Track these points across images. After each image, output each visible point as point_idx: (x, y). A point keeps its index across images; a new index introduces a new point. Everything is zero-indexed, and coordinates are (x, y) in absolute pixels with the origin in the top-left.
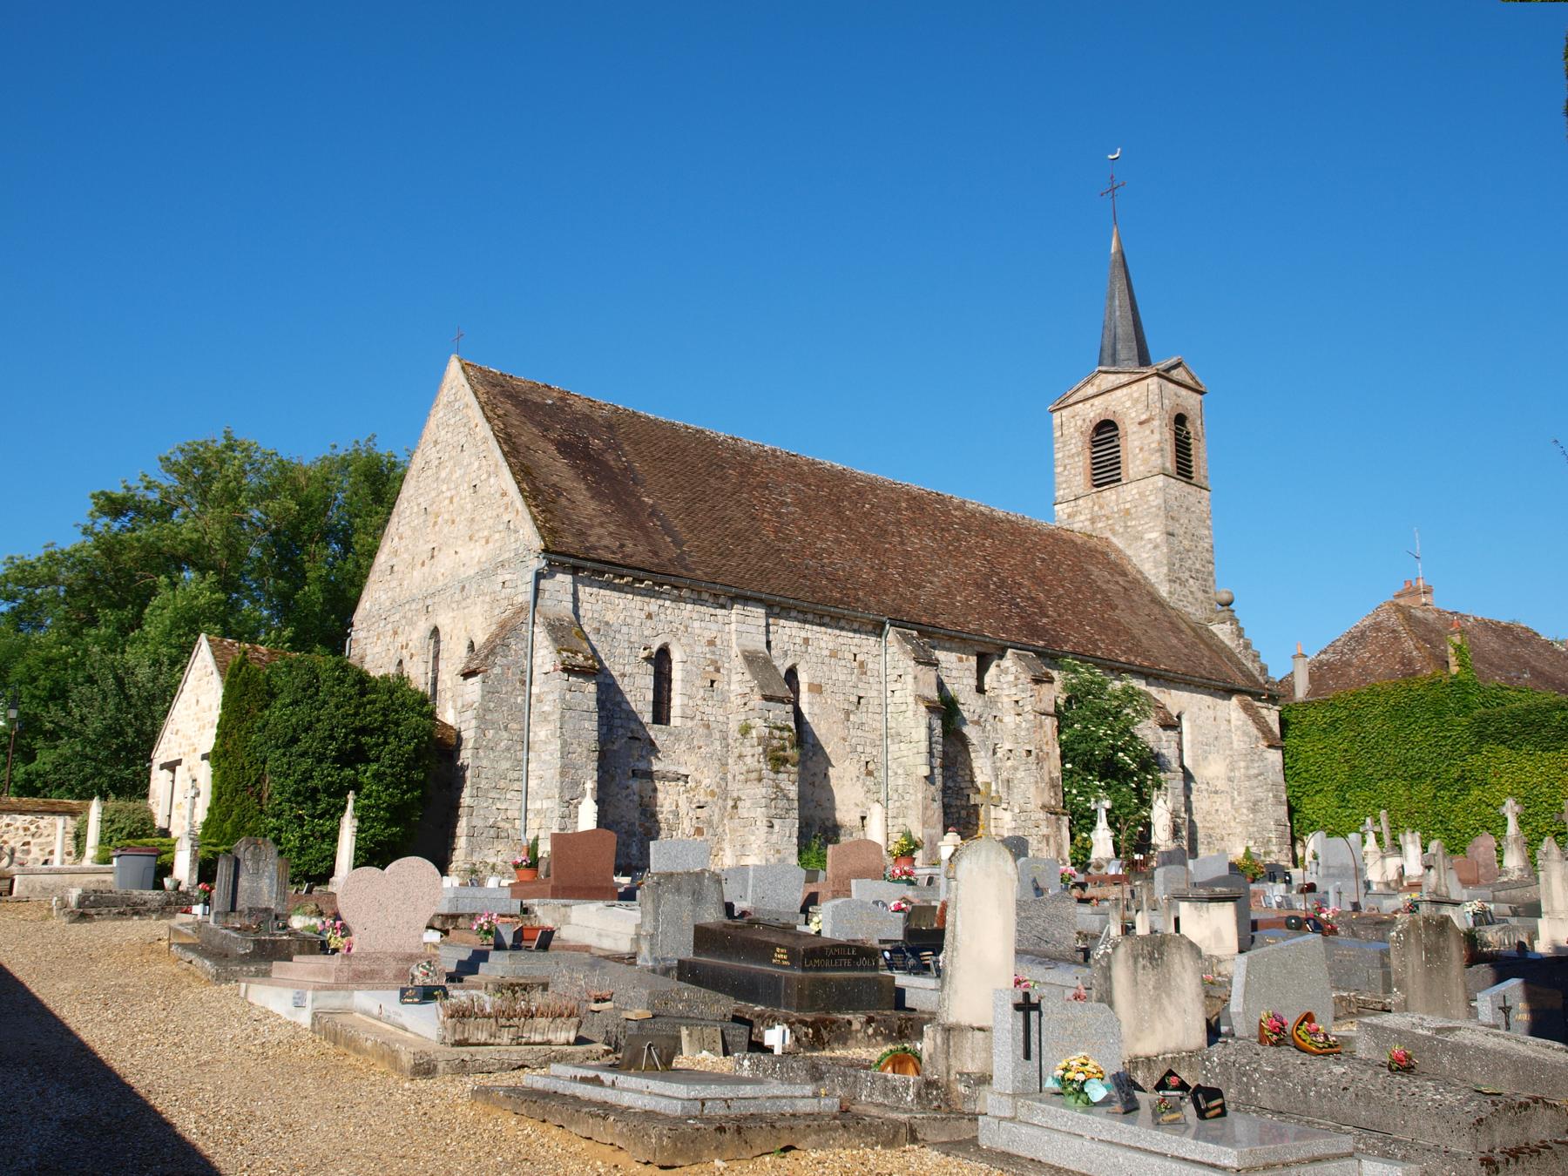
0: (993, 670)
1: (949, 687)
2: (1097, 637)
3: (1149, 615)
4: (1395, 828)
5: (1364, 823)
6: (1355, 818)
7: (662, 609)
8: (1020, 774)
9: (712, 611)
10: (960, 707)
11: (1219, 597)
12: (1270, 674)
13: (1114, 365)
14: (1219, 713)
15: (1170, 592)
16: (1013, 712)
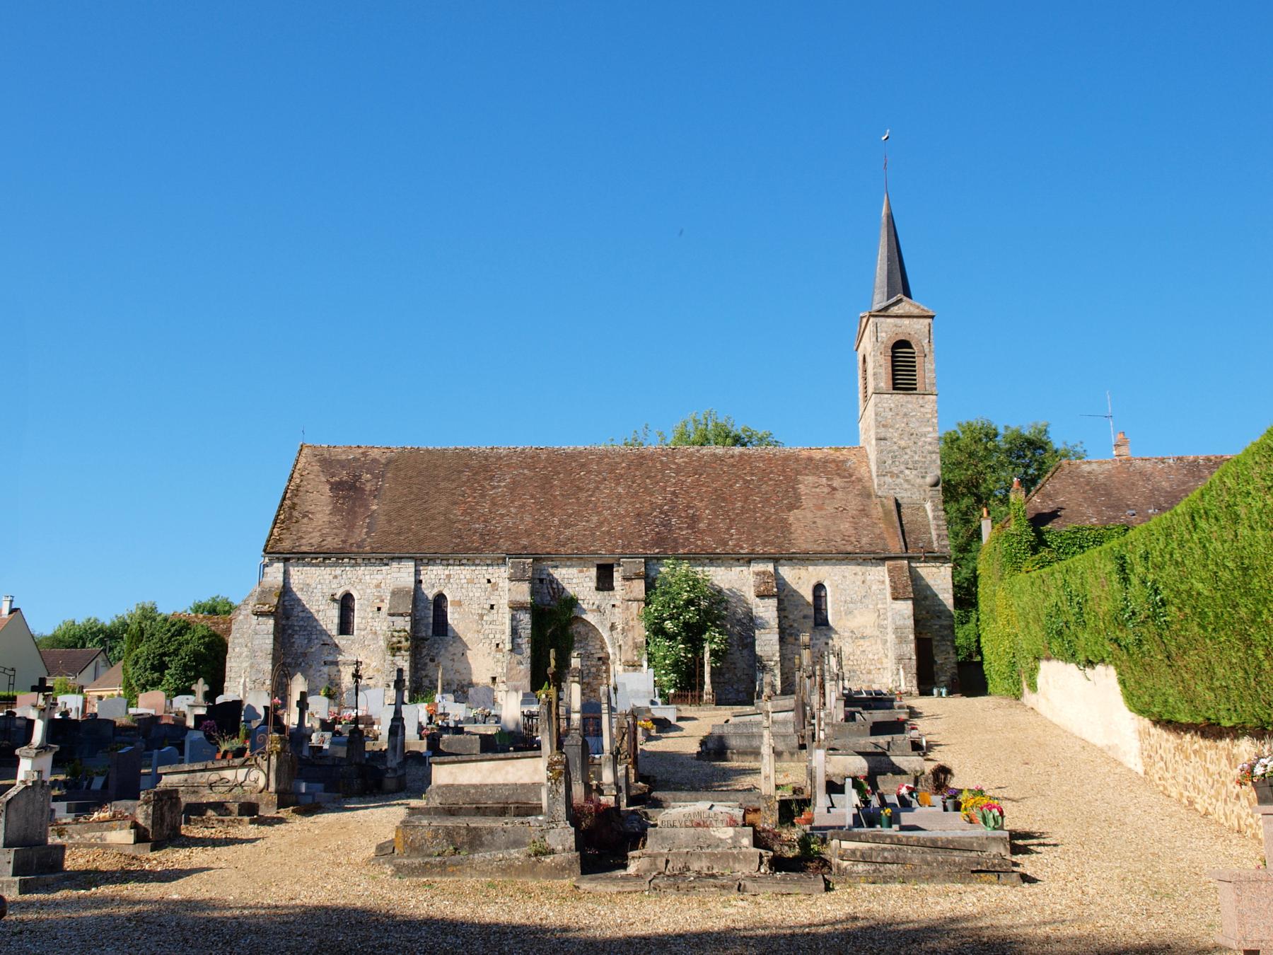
7: (344, 572)
9: (379, 568)
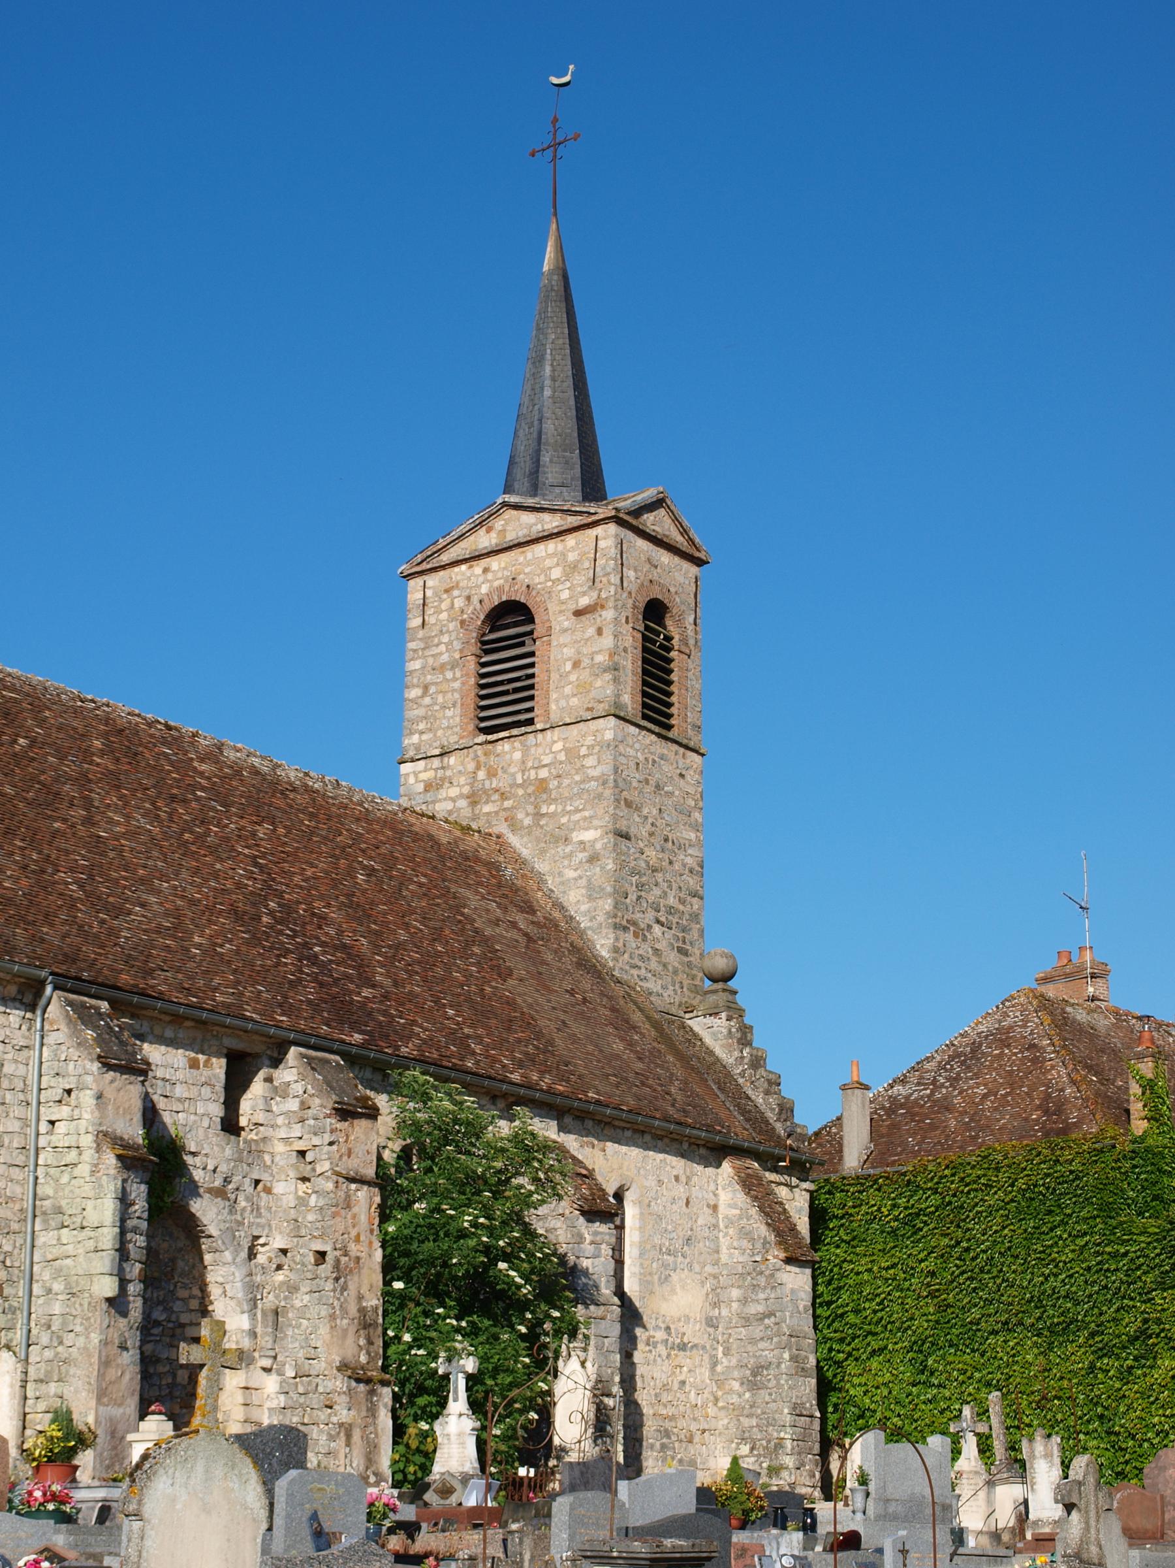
0: (257, 1087)
1: (167, 1118)
2: (466, 1031)
3: (571, 993)
4: (1016, 1427)
5: (958, 1417)
6: (943, 1405)
8: (301, 1299)
10: (189, 1159)
11: (708, 964)
12: (797, 1120)
13: (535, 495)
14: (695, 1192)
15: (616, 950)
16: (292, 1174)
